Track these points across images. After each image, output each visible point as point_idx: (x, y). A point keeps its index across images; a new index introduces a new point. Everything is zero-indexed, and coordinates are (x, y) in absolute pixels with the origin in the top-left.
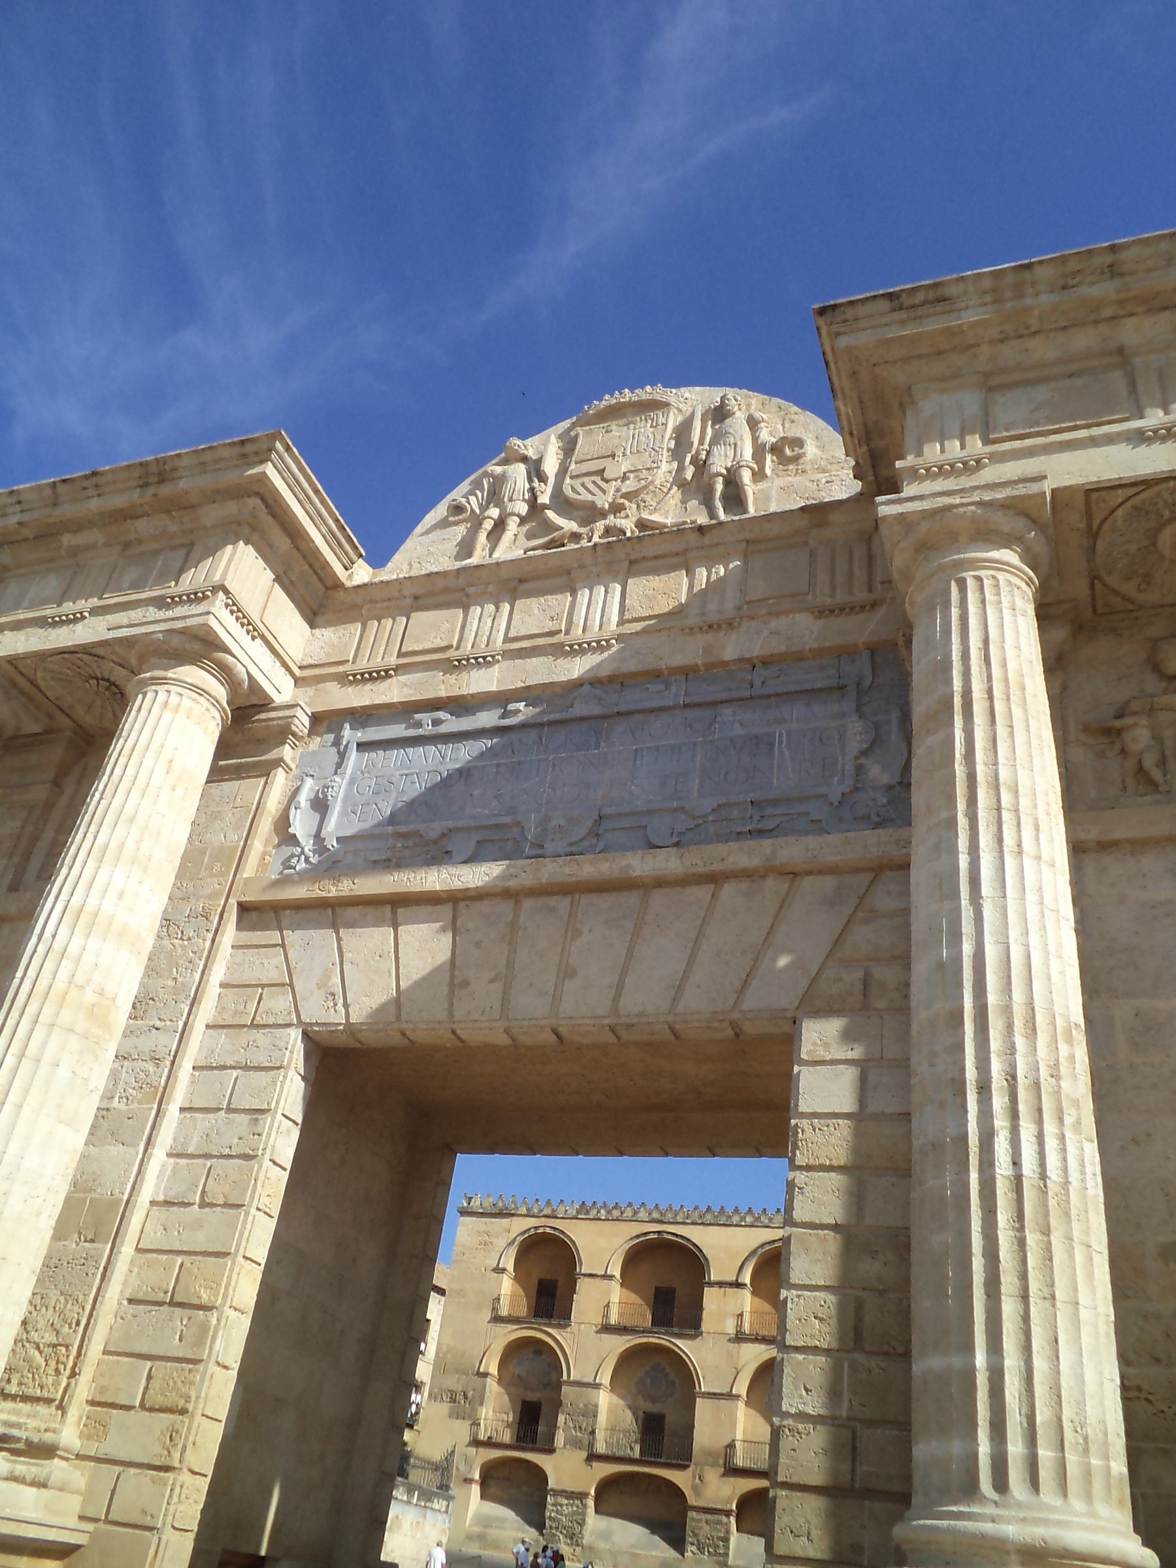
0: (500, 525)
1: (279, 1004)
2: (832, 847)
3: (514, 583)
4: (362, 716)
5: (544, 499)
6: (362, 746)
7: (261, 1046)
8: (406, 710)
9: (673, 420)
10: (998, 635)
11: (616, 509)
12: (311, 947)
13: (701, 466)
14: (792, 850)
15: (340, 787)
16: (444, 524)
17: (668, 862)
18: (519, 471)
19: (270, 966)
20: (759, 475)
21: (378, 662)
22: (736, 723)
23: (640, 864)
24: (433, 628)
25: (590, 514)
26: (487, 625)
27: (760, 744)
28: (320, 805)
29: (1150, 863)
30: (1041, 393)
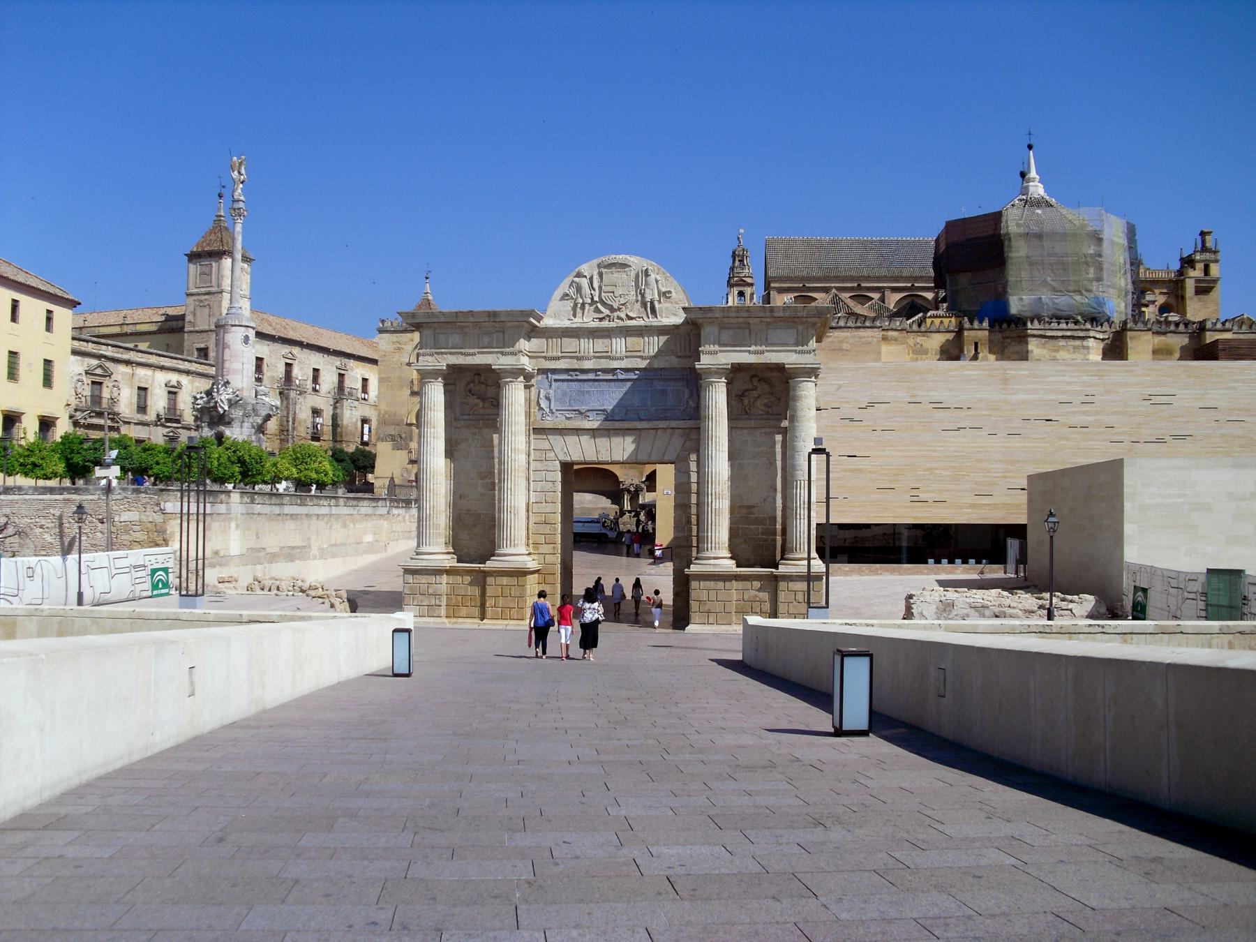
0: (583, 305)
1: (551, 455)
2: (682, 424)
3: (594, 333)
4: (554, 371)
5: (596, 299)
6: (556, 380)
7: (550, 465)
8: (567, 371)
9: (633, 274)
10: (718, 399)
11: (619, 309)
12: (557, 441)
13: (643, 296)
14: (674, 424)
15: (551, 392)
16: (562, 299)
17: (645, 425)
18: (585, 282)
19: (546, 445)
20: (660, 302)
21: (555, 354)
22: (659, 385)
23: (639, 425)
24: (570, 344)
25: (612, 309)
26: (586, 346)
27: (664, 392)
28: (548, 398)
29: (745, 431)
30: (731, 332)
